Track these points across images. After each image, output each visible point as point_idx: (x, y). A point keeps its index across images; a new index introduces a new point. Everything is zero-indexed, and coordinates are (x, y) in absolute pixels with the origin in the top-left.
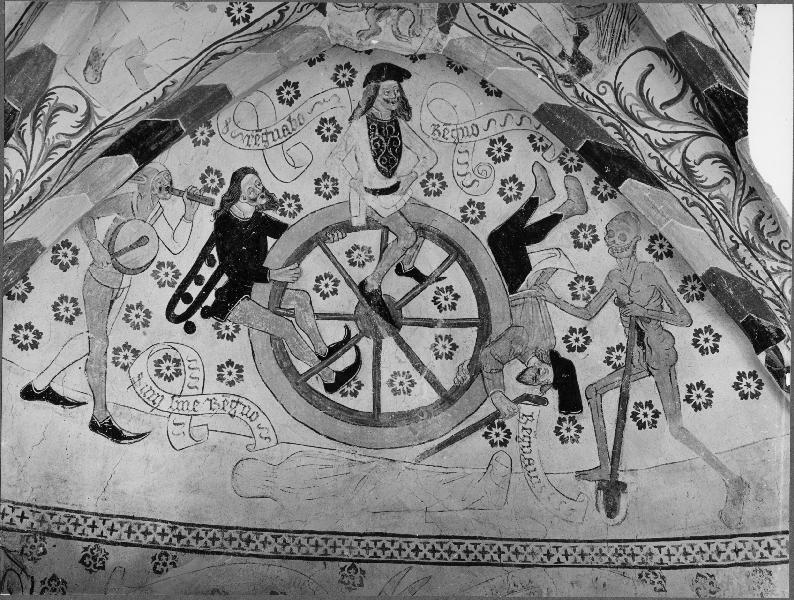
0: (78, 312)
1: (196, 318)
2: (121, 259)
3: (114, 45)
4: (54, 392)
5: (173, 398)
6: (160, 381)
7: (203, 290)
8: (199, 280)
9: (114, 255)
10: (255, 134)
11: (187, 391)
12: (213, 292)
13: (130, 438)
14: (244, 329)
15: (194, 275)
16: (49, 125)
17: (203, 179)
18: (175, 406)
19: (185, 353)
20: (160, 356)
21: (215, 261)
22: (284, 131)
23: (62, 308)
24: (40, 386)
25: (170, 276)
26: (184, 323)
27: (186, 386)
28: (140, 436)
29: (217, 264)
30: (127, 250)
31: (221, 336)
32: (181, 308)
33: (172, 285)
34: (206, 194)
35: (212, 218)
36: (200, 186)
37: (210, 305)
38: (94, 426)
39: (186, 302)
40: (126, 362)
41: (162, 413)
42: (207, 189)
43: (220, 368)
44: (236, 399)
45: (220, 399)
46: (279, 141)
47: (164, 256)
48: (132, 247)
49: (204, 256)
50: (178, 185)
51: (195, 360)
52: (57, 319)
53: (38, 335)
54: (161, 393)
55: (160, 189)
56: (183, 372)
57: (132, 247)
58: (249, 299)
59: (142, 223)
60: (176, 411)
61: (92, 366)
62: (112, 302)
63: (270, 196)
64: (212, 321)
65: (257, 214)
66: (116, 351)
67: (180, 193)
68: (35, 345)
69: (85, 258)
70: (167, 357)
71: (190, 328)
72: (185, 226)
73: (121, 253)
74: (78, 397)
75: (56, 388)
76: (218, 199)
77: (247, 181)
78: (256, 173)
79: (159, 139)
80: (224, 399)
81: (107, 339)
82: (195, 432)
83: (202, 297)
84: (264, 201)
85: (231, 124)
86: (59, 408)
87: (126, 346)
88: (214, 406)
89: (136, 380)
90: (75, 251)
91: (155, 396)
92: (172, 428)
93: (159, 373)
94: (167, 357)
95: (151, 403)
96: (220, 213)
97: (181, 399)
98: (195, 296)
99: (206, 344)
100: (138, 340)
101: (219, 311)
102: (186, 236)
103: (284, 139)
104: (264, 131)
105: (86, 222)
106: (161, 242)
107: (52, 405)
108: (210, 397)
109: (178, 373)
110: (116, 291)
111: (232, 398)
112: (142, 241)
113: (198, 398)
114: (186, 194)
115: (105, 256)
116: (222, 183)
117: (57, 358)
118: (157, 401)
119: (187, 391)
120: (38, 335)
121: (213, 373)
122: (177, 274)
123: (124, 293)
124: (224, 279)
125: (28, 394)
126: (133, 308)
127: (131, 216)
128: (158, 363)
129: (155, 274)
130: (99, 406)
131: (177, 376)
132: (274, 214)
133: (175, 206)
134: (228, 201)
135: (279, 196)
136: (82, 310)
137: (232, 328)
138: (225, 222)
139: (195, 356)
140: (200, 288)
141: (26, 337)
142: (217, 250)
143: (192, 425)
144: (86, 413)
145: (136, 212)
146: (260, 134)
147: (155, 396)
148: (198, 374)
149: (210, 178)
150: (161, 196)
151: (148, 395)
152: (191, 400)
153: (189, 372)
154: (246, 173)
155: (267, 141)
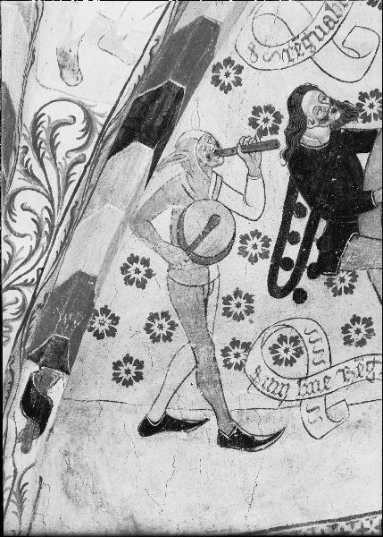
0: (173, 326)
1: (304, 282)
2: (199, 251)
3: (76, 37)
4: (173, 419)
5: (299, 383)
6: (282, 369)
7: (302, 248)
8: (293, 238)
9: (188, 249)
10: (292, 44)
11: (313, 369)
12: (314, 244)
13: (265, 442)
14: (362, 274)
15: (286, 235)
16: (53, 147)
17: (253, 123)
18: (303, 392)
19: (301, 326)
20: (274, 340)
21: (305, 209)
22: (327, 24)
23: (155, 328)
24: (156, 417)
25: (260, 246)
26: (291, 295)
27: (311, 362)
28: (274, 437)
29: (309, 211)
30: (201, 238)
31: (337, 293)
32: (284, 277)
33: (264, 255)
34: (264, 139)
35: (284, 162)
36: (253, 132)
37: (315, 261)
38: (223, 442)
39: (287, 269)
40: (238, 361)
41: (294, 403)
43: (345, 329)
44: (371, 358)
45: (352, 365)
46: (327, 38)
47: (244, 228)
48: (205, 233)
49: (290, 209)
50: (225, 145)
51: (315, 331)
52: (154, 342)
53: (140, 364)
54: (286, 381)
55: (208, 157)
56: (304, 349)
57: (205, 233)
58: (358, 236)
60: (307, 396)
61: (207, 378)
62: (206, 301)
63: (344, 106)
64: (323, 278)
65: (335, 134)
66: (225, 352)
67: (233, 151)
68: (139, 377)
69: (158, 265)
70: (282, 339)
71: (301, 297)
72: (255, 185)
73: (195, 244)
74: (197, 416)
75: (175, 414)
76: (281, 137)
77: (308, 103)
78: (315, 88)
79: (158, 111)
80: (357, 363)
81: (212, 343)
82: (332, 412)
83: (303, 256)
84: (338, 115)
85: (259, 50)
86: (182, 434)
87: (235, 343)
88: (347, 376)
89: (254, 376)
90: (146, 262)
91: (280, 387)
92: (306, 416)
93: (278, 361)
94: (282, 339)
95: (277, 396)
96: (291, 152)
97: (309, 380)
98: (294, 258)
99: (327, 308)
100: (245, 330)
101: (328, 265)
102: (261, 194)
103: (332, 32)
104: (302, 36)
105: (139, 221)
106: (234, 214)
107: (173, 433)
108: (342, 367)
109: (299, 353)
110: (206, 287)
111: (367, 359)
112: (213, 222)
113: (327, 373)
115: (180, 255)
116: (278, 117)
117: (170, 380)
118: (283, 393)
119: (313, 369)
120: (140, 364)
121: (337, 337)
122: (266, 242)
123: (216, 285)
124: (323, 224)
125: (147, 429)
126: (231, 299)
127: (189, 200)
128: (274, 349)
129: (243, 252)
130: (222, 418)
131: (298, 356)
132: (358, 125)
133: (234, 168)
134: (295, 133)
135: (354, 101)
136: (177, 321)
137: (348, 279)
138: (298, 159)
139: (311, 326)
140: (298, 246)
141: (128, 372)
142: (305, 197)
143: (328, 407)
144: (212, 428)
145: (192, 194)
146: (298, 41)
147: (280, 387)
148: (322, 345)
150: (212, 164)
151: (271, 389)
152: (320, 377)
153: (310, 347)
154: (303, 93)
155: (311, 45)
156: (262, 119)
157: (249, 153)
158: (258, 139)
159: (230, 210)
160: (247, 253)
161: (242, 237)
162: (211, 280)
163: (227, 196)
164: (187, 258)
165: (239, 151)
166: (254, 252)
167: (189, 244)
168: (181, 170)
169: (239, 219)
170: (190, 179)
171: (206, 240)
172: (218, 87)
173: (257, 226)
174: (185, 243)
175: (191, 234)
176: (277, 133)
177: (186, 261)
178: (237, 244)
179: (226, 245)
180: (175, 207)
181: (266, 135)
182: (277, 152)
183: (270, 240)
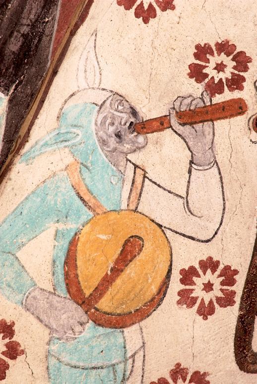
2: (105, 304)
9: (86, 302)
17: (197, 73)
25: (217, 286)
30: (107, 281)
33: (227, 300)
34: (218, 99)
36: (196, 89)
42: (215, 88)
47: (187, 255)
48: (117, 271)
50: (149, 111)
55: (118, 136)
57: (117, 271)
59: (113, 216)
67: (162, 123)
72: (205, 183)
106: (168, 233)
112: (130, 249)
114: (174, 121)
122: (229, 276)
123: (139, 363)
129: (186, 299)
133: (165, 153)
149: (212, 64)
150: (127, 147)
156: (212, 64)
157: (191, 124)
158: (207, 99)
159: (160, 226)
160: (194, 301)
161: (183, 272)
162: (129, 354)
163: (158, 206)
164: (84, 318)
165: (174, 121)
166: (207, 297)
167: (87, 293)
168: (69, 160)
169: (178, 243)
170: (86, 174)
171: (118, 281)
172: (133, 10)
173: (211, 251)
174: (80, 290)
175: (89, 275)
176: (241, 88)
177: (82, 324)
178: (176, 285)
179: (154, 289)
180: (61, 226)
181: (221, 91)
182: (240, 122)
183: (236, 272)
